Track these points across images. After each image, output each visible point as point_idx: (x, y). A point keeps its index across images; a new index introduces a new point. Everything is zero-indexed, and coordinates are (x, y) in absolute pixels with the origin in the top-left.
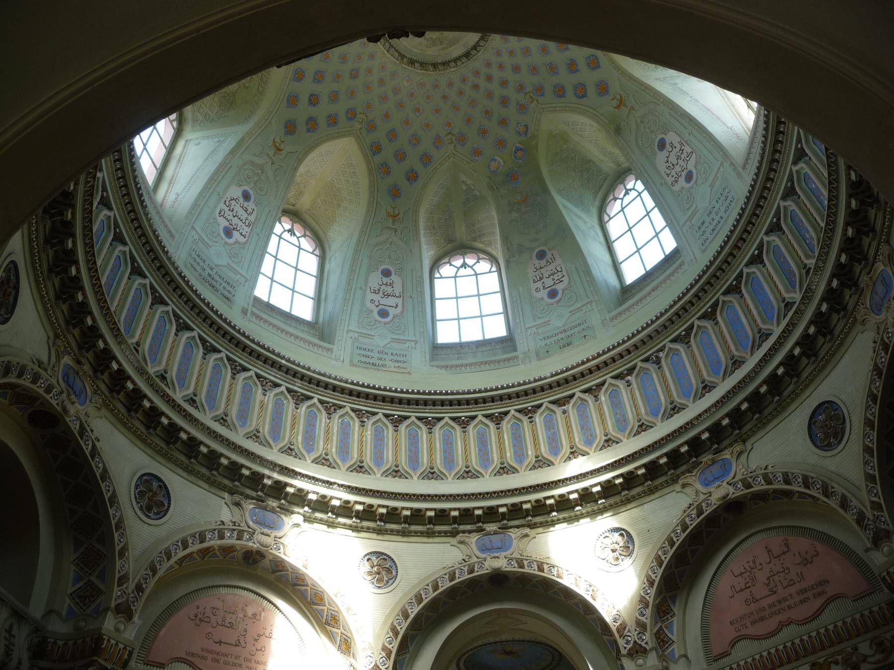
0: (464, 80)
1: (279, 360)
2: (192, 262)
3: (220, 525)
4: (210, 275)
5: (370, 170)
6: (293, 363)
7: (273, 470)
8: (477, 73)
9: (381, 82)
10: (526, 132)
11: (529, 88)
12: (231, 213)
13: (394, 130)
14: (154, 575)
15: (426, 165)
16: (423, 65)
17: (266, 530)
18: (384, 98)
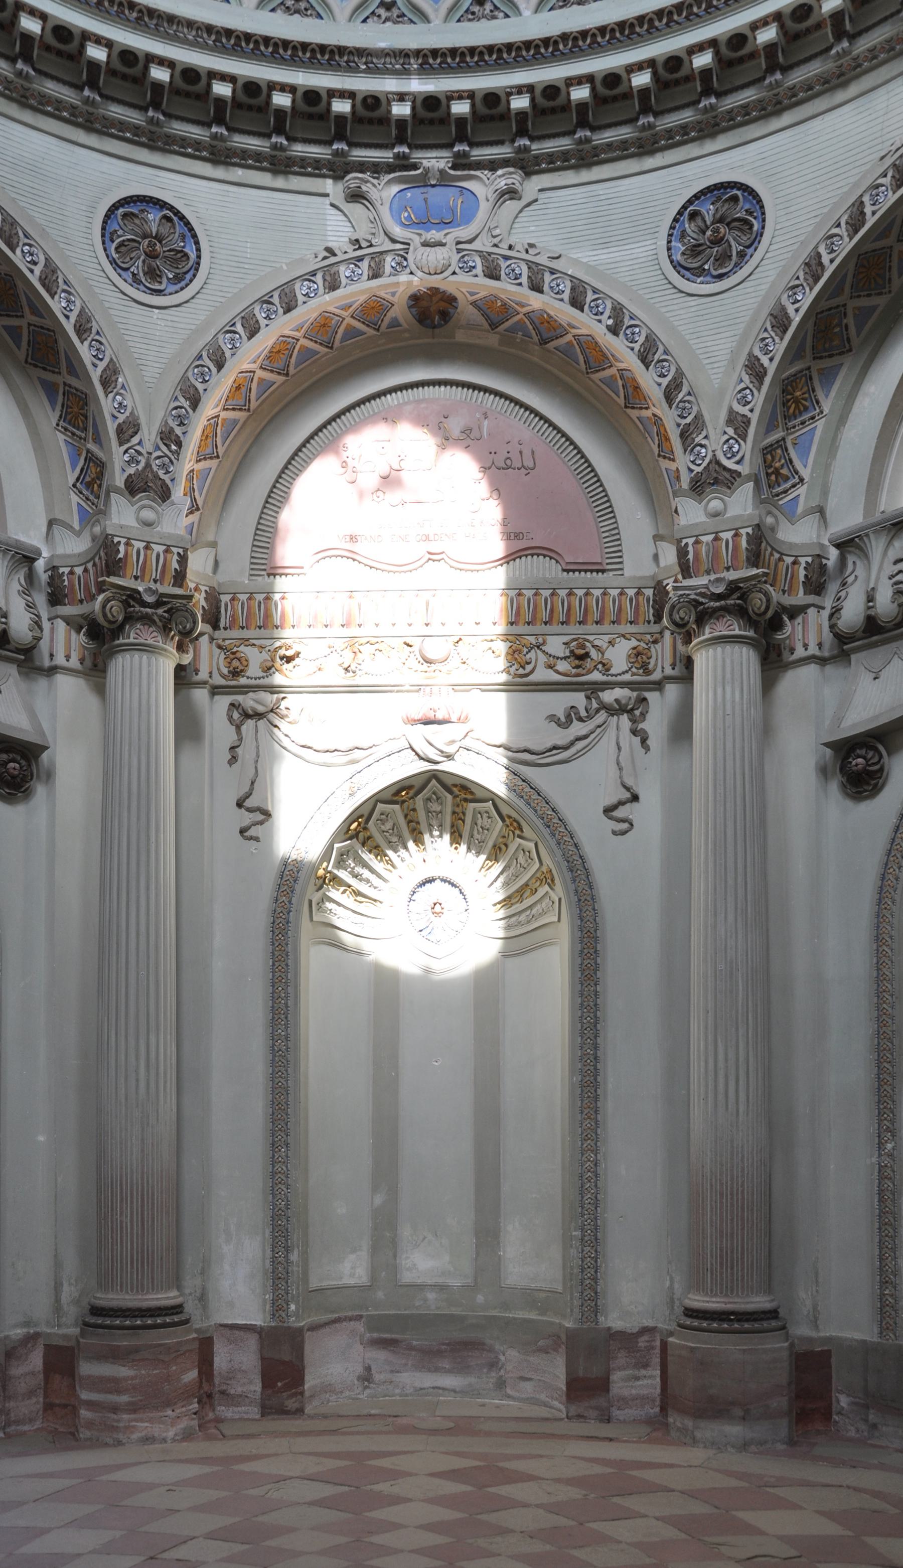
3: (325, 258)
7: (405, 72)
17: (434, 235)
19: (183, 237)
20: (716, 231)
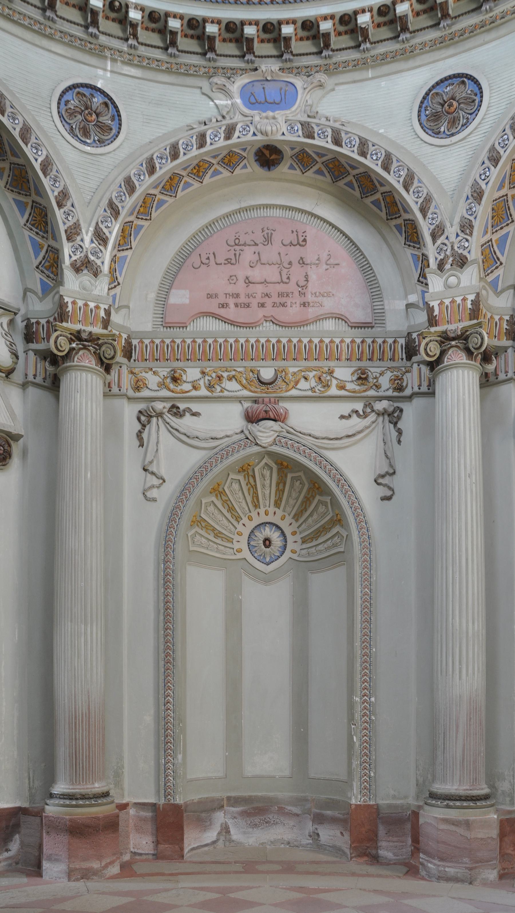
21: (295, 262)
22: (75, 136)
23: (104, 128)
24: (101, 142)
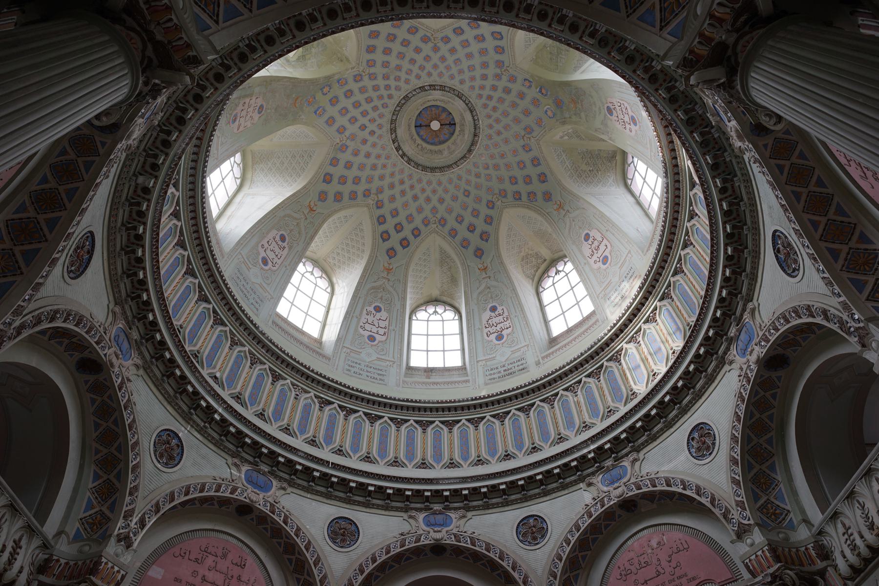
0: (489, 117)
1: (564, 369)
2: (490, 377)
4: (505, 371)
5: (528, 208)
6: (571, 362)
7: (588, 446)
8: (485, 106)
9: (478, 176)
10: (529, 81)
11: (498, 71)
12: (493, 327)
13: (510, 178)
14: (555, 579)
15: (539, 164)
16: (473, 143)
17: (616, 485)
18: (489, 178)
19: (542, 523)
20: (701, 441)
21: (235, 577)
22: (155, 456)
23: (171, 458)
24: (166, 465)
